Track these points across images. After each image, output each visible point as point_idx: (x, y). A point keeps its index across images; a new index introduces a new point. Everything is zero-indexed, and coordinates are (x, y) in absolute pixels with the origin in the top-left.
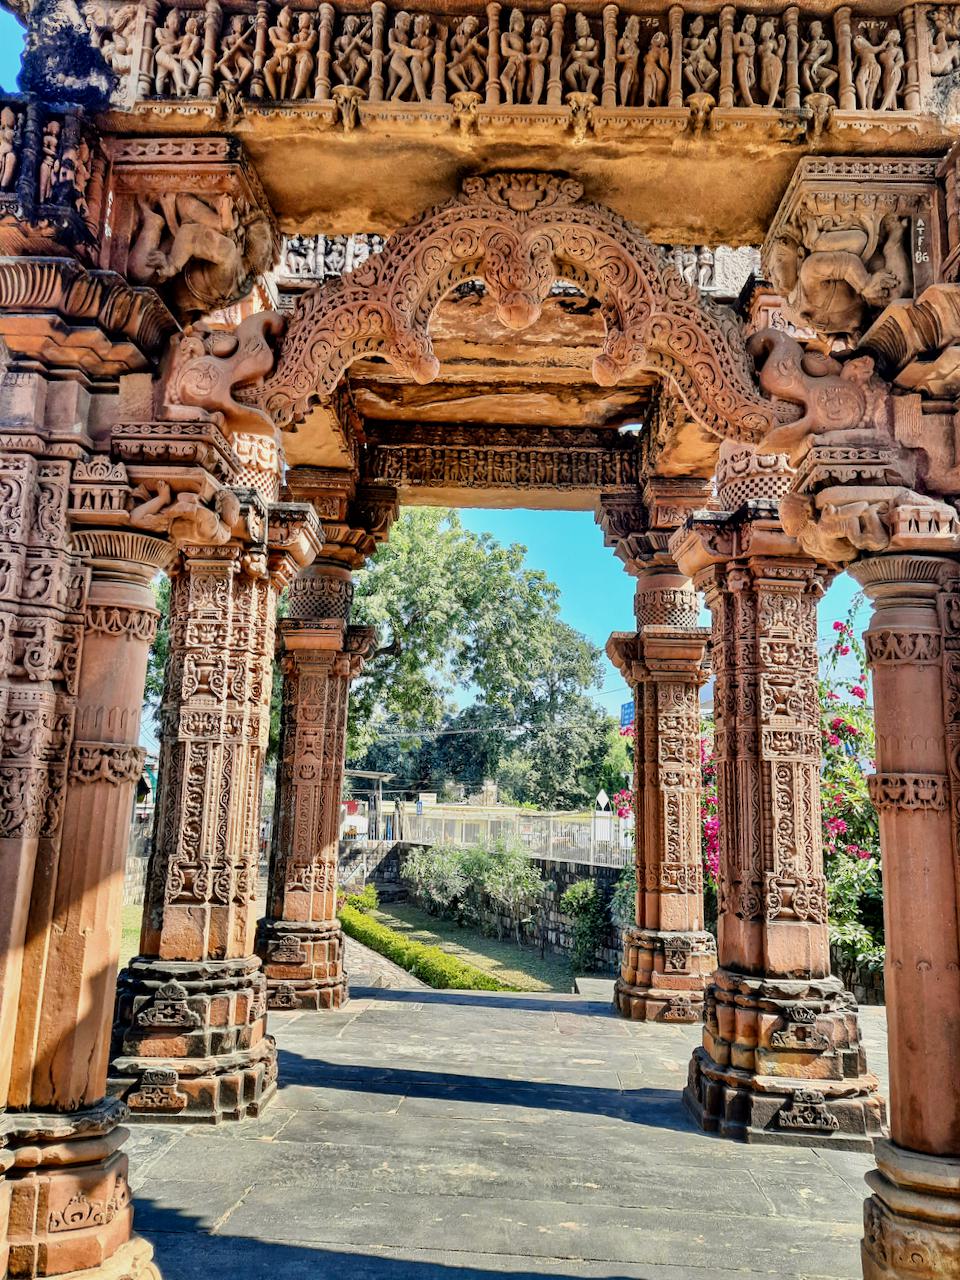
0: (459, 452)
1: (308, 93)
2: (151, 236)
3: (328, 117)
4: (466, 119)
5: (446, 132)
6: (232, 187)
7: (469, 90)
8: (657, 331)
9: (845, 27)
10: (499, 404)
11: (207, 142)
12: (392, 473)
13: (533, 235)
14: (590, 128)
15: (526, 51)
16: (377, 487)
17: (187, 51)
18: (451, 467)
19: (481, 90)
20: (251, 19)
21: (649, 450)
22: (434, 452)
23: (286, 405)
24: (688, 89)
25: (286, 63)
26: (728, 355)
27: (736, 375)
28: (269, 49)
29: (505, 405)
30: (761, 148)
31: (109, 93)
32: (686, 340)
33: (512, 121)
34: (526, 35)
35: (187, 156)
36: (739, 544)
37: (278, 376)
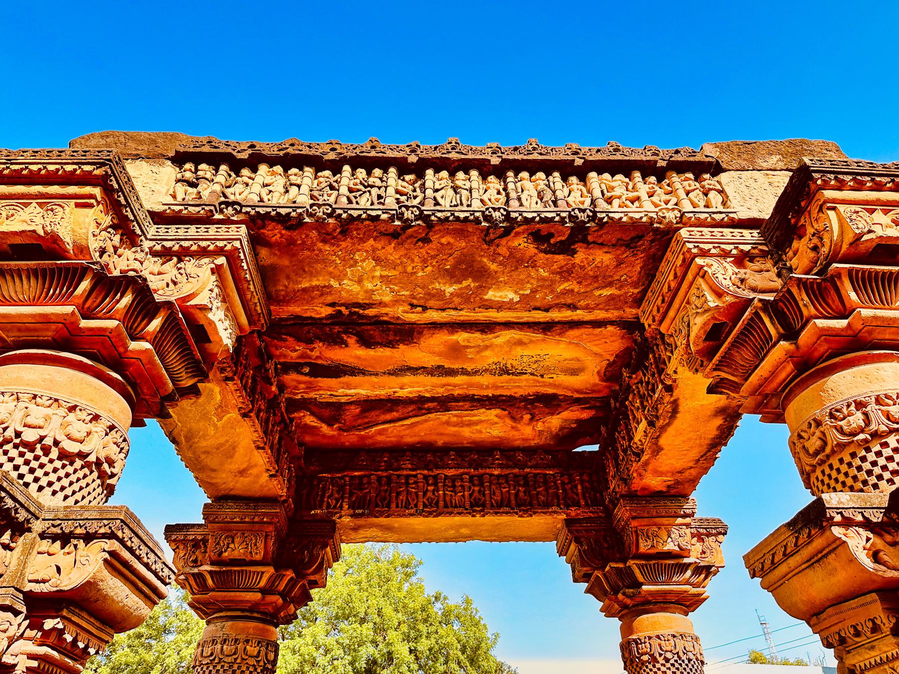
0: (407, 477)
10: (448, 423)
12: (333, 502)
16: (316, 519)
18: (398, 494)
21: (617, 465)
22: (379, 478)
29: (456, 425)
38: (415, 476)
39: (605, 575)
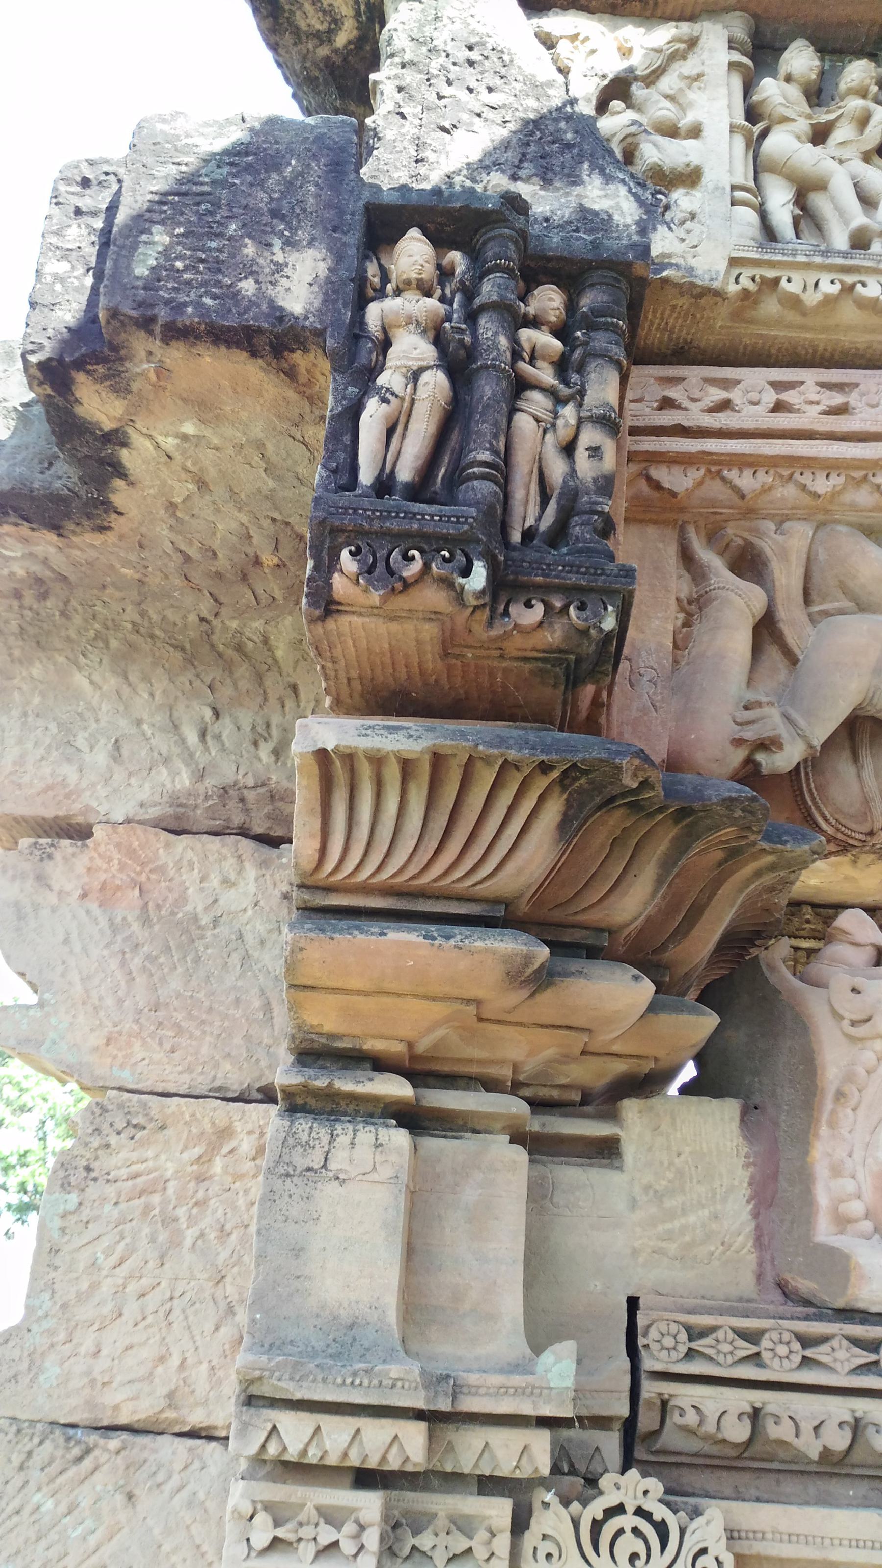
2: (730, 639)
31: (644, 229)
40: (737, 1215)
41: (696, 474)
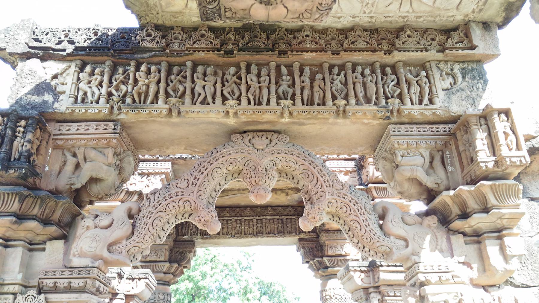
0: (227, 220)
1: (155, 101)
3: (165, 112)
4: (232, 112)
5: (223, 117)
6: (114, 145)
7: (233, 99)
8: (330, 205)
9: (402, 71)
11: (102, 124)
13: (266, 161)
14: (291, 114)
15: (259, 83)
17: (94, 83)
19: (239, 99)
20: (127, 68)
23: (138, 252)
24: (334, 98)
25: (144, 88)
26: (366, 216)
27: (371, 227)
28: (136, 81)
30: (370, 121)
31: (53, 103)
32: (345, 209)
33: (254, 112)
34: (259, 76)
35: (92, 130)
36: (374, 279)
37: (134, 237)
38: (230, 220)
39: (314, 263)
40: (61, 256)
41: (63, 141)
